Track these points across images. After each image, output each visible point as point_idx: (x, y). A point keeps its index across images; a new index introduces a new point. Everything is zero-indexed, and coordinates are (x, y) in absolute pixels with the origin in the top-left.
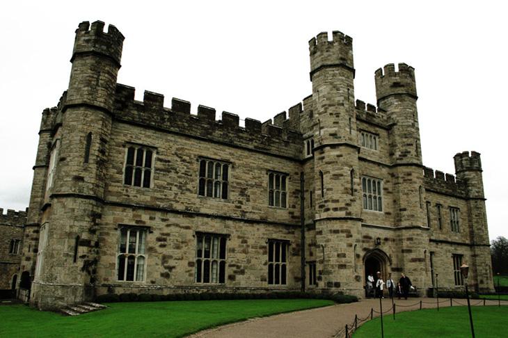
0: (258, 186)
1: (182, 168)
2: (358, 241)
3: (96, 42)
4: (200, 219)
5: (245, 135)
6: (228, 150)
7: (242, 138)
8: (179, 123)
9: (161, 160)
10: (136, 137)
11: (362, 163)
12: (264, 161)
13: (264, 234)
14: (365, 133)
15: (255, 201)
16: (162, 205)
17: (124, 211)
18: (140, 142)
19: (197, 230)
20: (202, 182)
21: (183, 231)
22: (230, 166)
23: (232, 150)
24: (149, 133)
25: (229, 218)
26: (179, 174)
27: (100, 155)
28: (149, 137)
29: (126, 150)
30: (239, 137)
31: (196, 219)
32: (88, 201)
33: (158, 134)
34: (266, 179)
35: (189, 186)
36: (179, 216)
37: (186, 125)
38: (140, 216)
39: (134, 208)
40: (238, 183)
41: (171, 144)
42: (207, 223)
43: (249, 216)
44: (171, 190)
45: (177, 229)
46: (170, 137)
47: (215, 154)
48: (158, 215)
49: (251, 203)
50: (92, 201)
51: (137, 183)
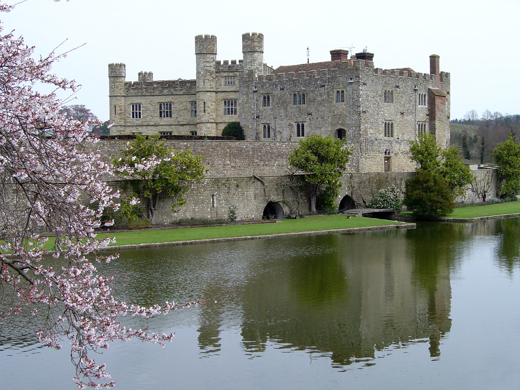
0: (185, 109)
1: (152, 108)
2: (205, 131)
3: (112, 72)
4: (160, 126)
5: (179, 88)
6: (171, 97)
7: (177, 90)
8: (150, 91)
9: (143, 107)
10: (134, 101)
11: (223, 93)
12: (188, 98)
13: (189, 129)
14: (227, 78)
15: (184, 116)
16: (145, 124)
17: (132, 128)
18: (135, 102)
19: (160, 131)
20: (161, 113)
21: (154, 132)
22: (172, 103)
23: (173, 97)
24: (139, 98)
25: (172, 125)
26: (151, 111)
27: (119, 111)
28: (138, 99)
29: (131, 106)
30: (175, 90)
31: (159, 127)
32: (117, 127)
33: (142, 97)
34: (189, 106)
35: (155, 115)
36: (152, 126)
37: (152, 91)
38: (138, 129)
39: (136, 126)
40: (177, 110)
41: (147, 100)
42: (163, 128)
43: (181, 123)
44: (148, 117)
45: (152, 131)
46: (147, 97)
47: (165, 100)
48: (145, 127)
49: (182, 117)
50: (119, 127)
51: (137, 117)
